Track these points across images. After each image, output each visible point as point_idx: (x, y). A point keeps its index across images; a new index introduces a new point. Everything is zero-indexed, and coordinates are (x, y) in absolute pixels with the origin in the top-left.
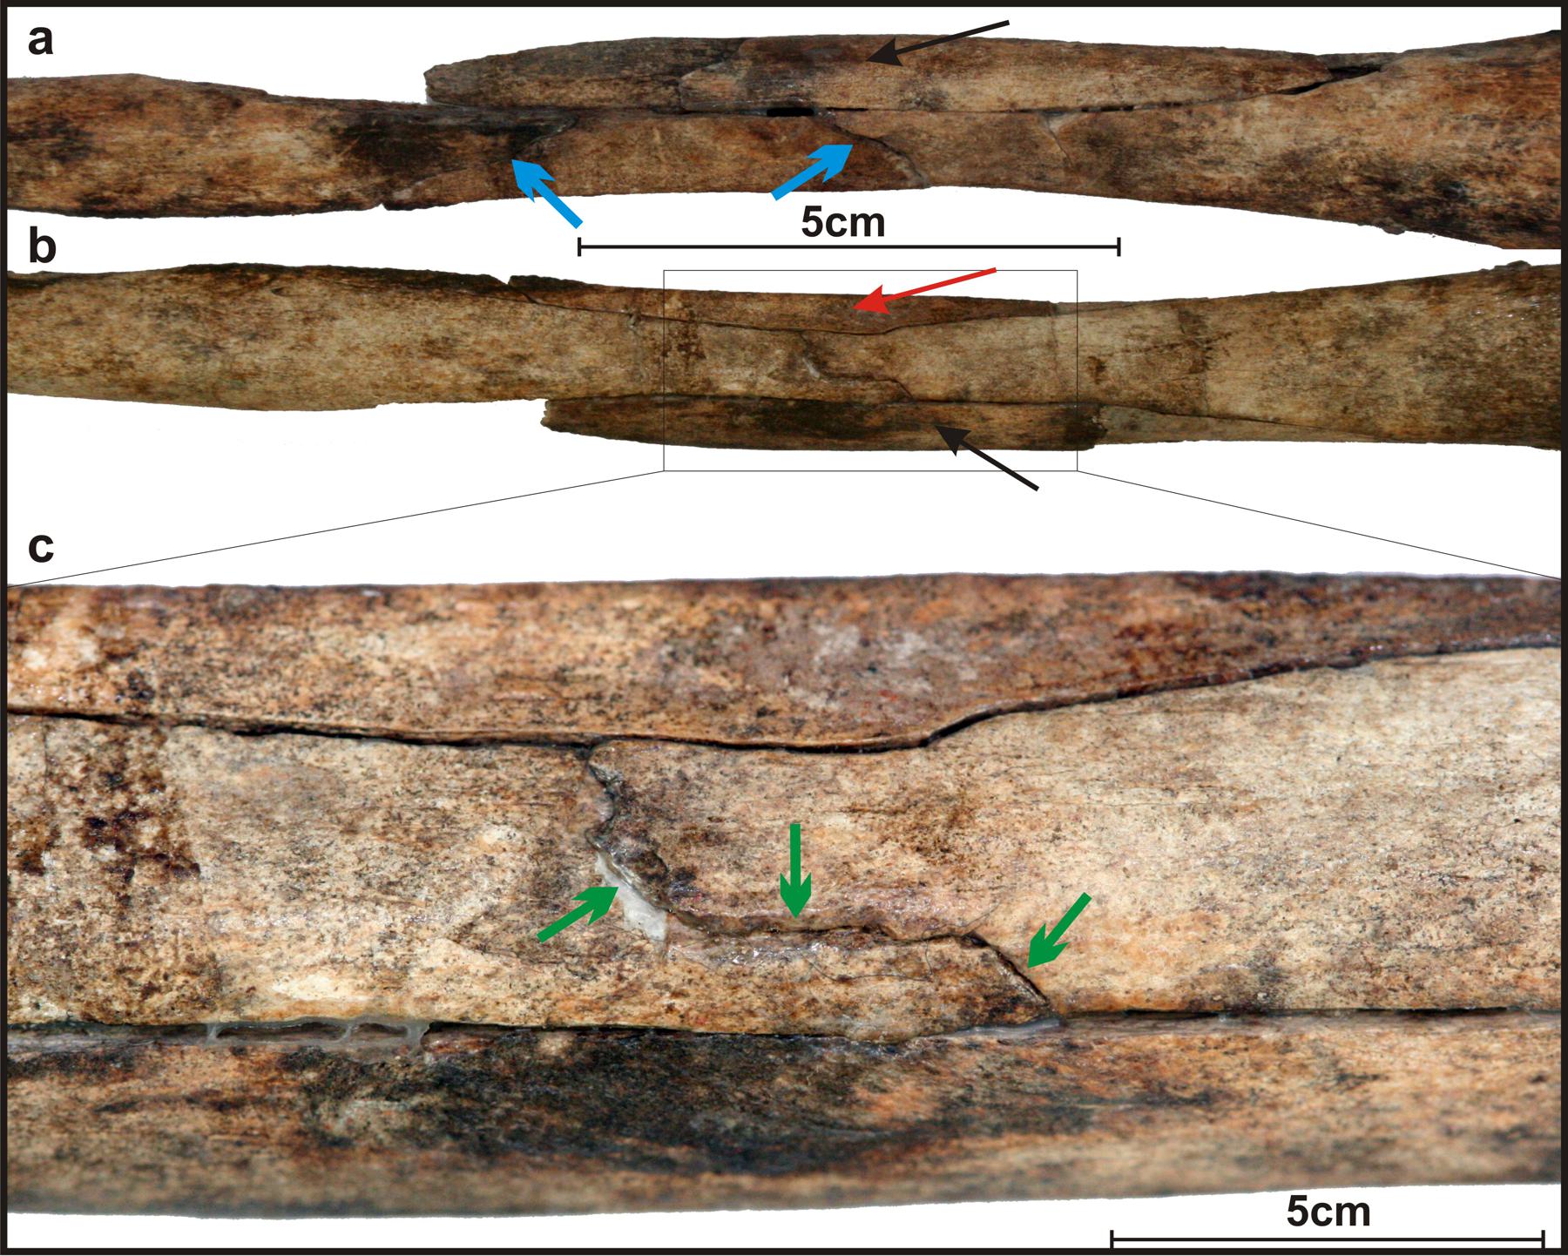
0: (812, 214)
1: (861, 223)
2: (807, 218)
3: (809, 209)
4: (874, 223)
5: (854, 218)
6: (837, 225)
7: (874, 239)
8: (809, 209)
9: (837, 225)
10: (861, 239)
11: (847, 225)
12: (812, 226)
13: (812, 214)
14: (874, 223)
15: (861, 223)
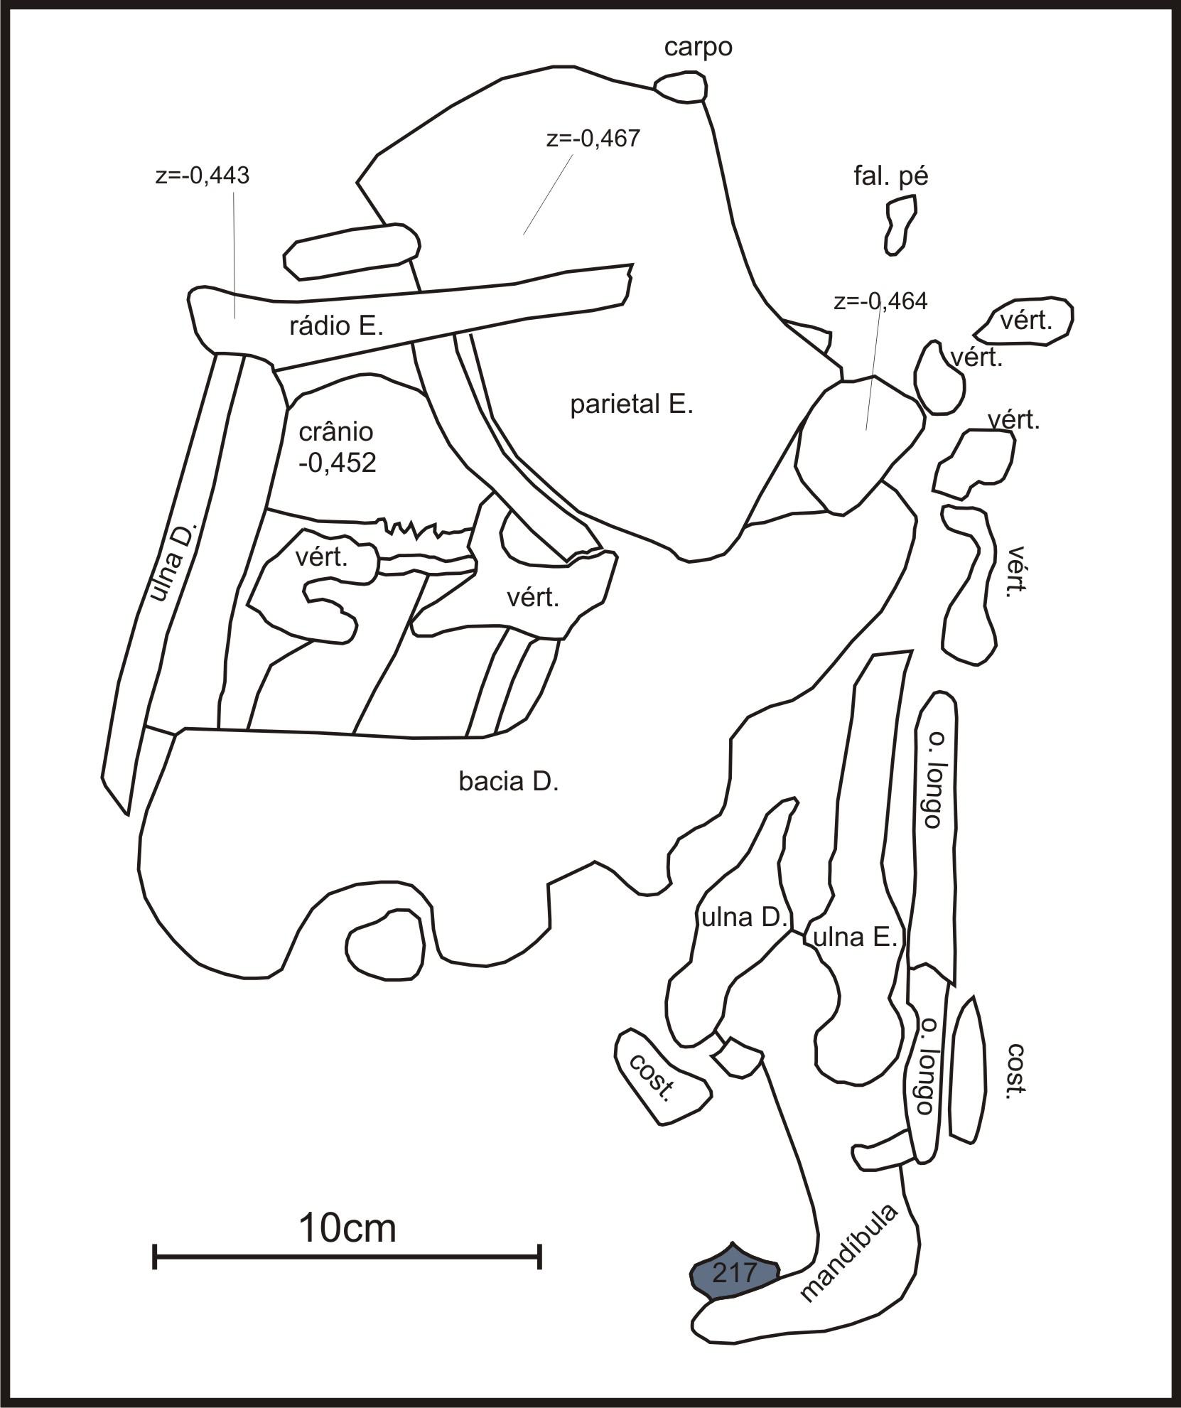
1: (374, 1228)
4: (387, 1228)
5: (368, 1224)
6: (354, 1231)
9: (354, 1231)
11: (363, 1230)
14: (387, 1228)
15: (374, 1228)
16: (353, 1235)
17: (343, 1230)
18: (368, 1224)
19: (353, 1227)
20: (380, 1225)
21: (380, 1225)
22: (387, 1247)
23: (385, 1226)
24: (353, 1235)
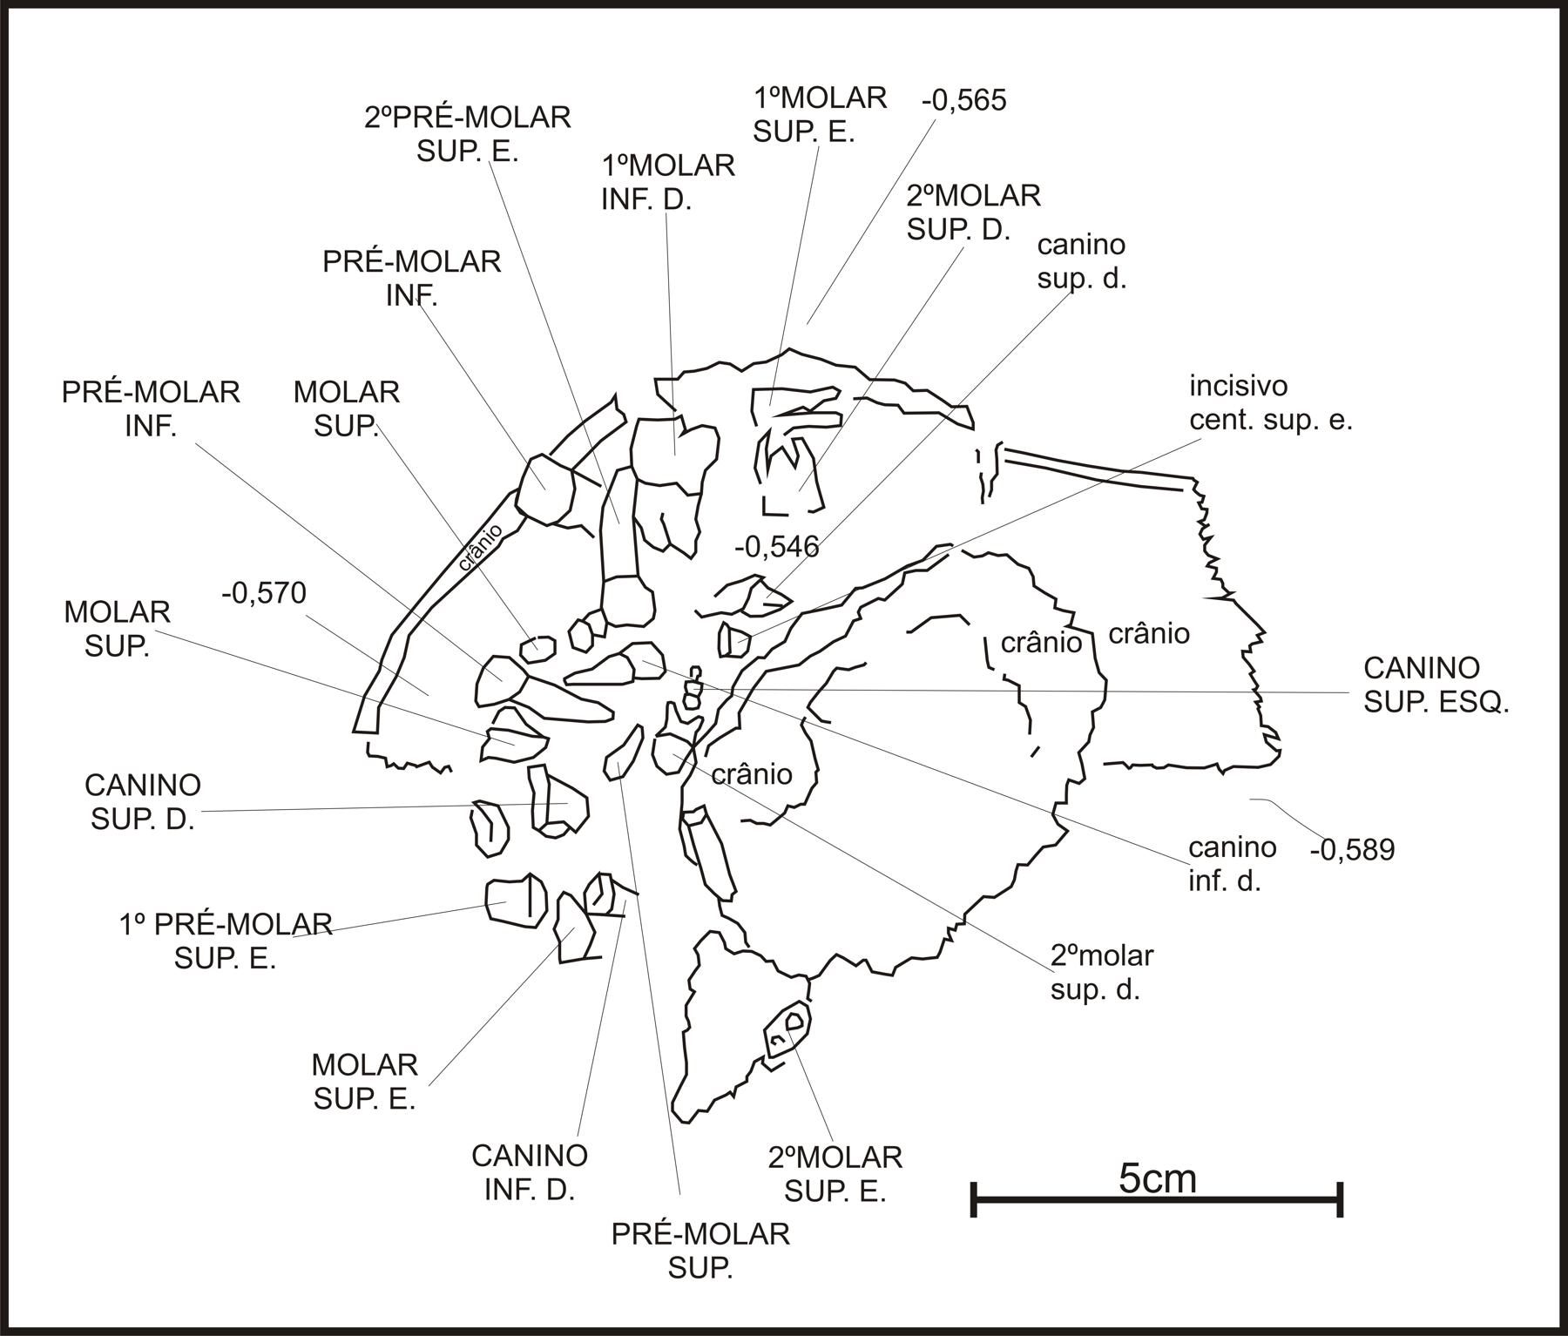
0: (1129, 1169)
1: (1174, 1178)
2: (1123, 1176)
3: (1125, 1165)
4: (1187, 1179)
5: (1168, 1174)
6: (1154, 1182)
7: (1187, 1192)
8: (1125, 1165)
9: (1154, 1182)
10: (1174, 1192)
11: (1162, 1181)
12: (1130, 1183)
13: (1129, 1169)
14: (1187, 1179)
15: (1174, 1178)
16: (1153, 1186)
18: (1168, 1174)
19: (1153, 1177)
20: (1181, 1175)
21: (1181, 1175)
24: (1153, 1186)
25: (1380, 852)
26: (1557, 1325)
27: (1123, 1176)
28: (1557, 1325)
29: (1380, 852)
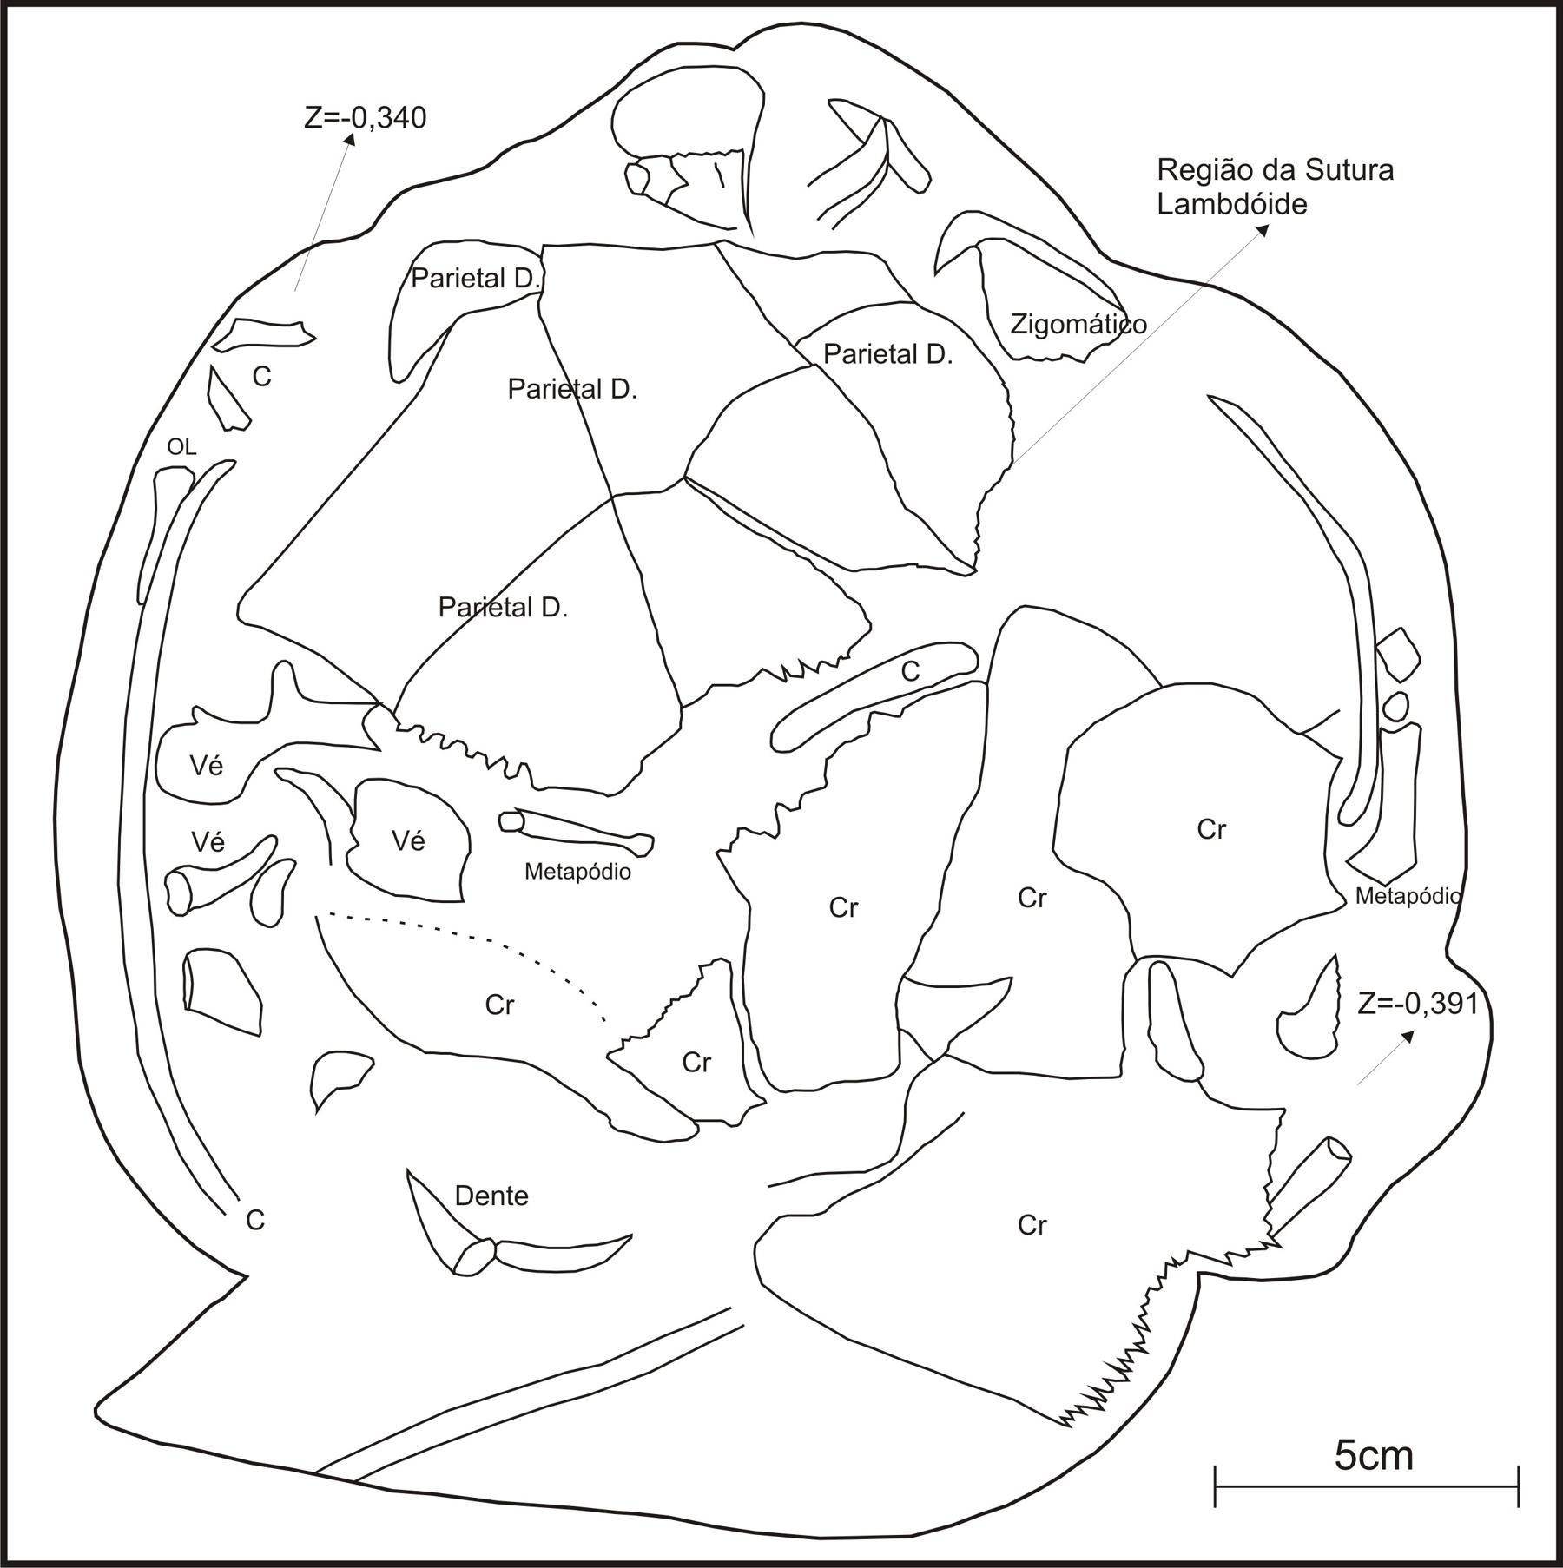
0: (1345, 1446)
1: (1391, 1455)
2: (1339, 1452)
3: (1341, 1442)
4: (1404, 1455)
5: (1385, 1451)
8: (1341, 1442)
9: (1370, 1458)
11: (1379, 1458)
12: (1346, 1459)
13: (1345, 1446)
14: (1404, 1455)
15: (1391, 1455)
16: (1369, 1463)
17: (1358, 1459)
18: (1385, 1451)
19: (1370, 1452)
20: (1397, 1452)
21: (1397, 1452)
22: (1403, 1476)
23: (1401, 1454)
24: (1369, 1463)
25: (1448, 1006)
26: (1554, 1558)
27: (1339, 1452)
28: (1554, 1558)
29: (1448, 1006)
